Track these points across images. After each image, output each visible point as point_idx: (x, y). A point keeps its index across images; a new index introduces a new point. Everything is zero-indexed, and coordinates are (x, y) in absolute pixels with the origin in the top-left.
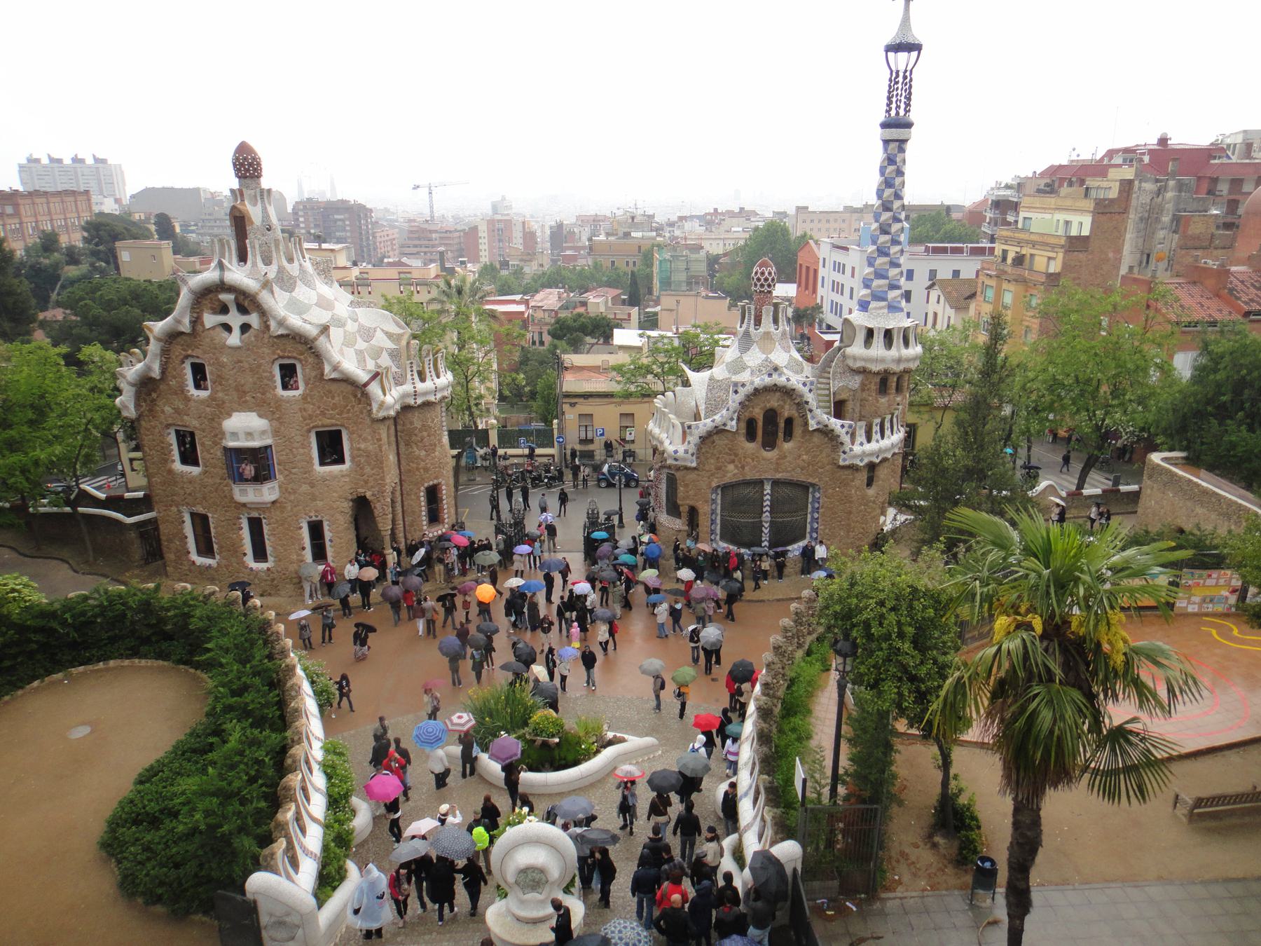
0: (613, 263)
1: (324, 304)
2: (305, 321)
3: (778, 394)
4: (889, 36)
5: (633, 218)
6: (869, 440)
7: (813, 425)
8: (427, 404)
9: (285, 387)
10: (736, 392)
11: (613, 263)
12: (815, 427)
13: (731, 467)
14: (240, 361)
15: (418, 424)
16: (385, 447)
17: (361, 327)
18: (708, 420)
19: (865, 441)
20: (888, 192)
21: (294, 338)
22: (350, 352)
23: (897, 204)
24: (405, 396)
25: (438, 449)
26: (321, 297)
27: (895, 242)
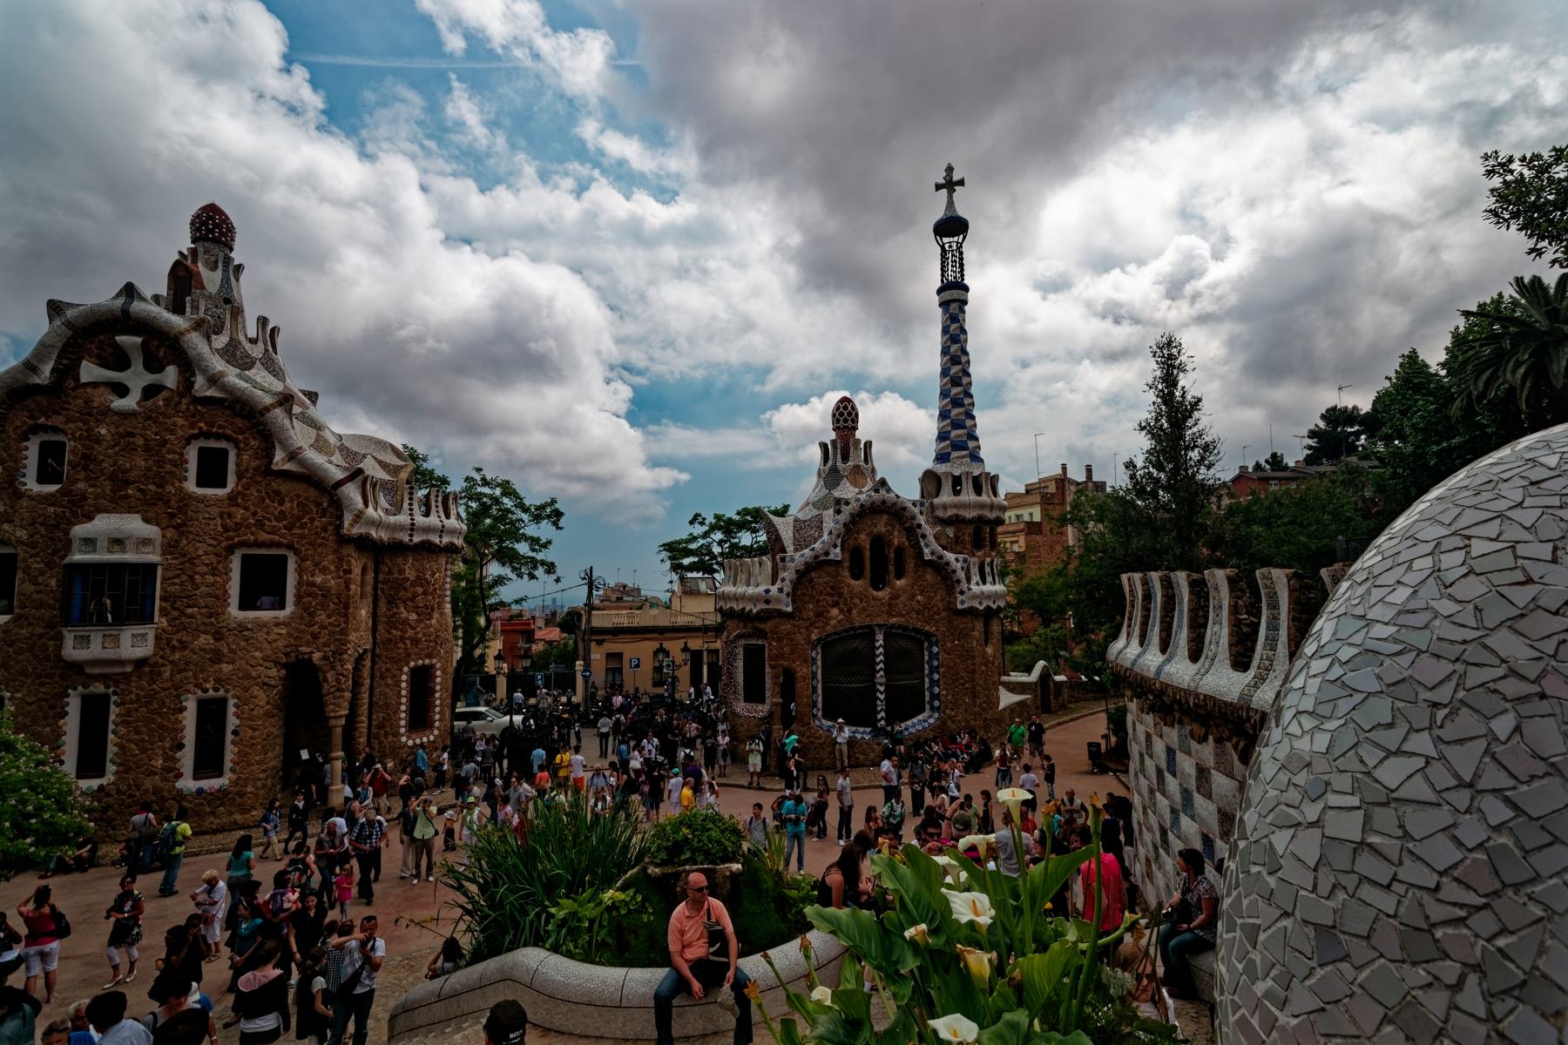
8: (427, 549)
9: (201, 483)
13: (835, 612)
14: (132, 435)
15: (410, 574)
18: (806, 551)
21: (231, 407)
25: (436, 615)
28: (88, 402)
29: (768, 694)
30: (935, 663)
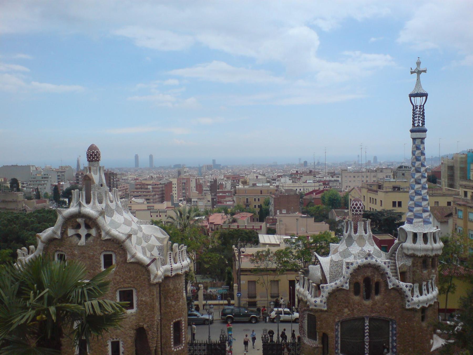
0: (247, 199)
1: (127, 223)
2: (119, 232)
3: (371, 269)
4: (411, 91)
5: (257, 177)
6: (421, 295)
7: (391, 286)
8: (177, 275)
10: (348, 268)
11: (247, 199)
12: (392, 287)
13: (346, 310)
14: (84, 253)
15: (171, 287)
16: (155, 299)
17: (144, 234)
18: (333, 284)
19: (419, 295)
20: (418, 163)
22: (139, 248)
23: (423, 169)
24: (166, 271)
25: (181, 300)
26: (125, 219)
27: (424, 188)
28: (71, 242)
29: (318, 337)
30: (395, 332)
